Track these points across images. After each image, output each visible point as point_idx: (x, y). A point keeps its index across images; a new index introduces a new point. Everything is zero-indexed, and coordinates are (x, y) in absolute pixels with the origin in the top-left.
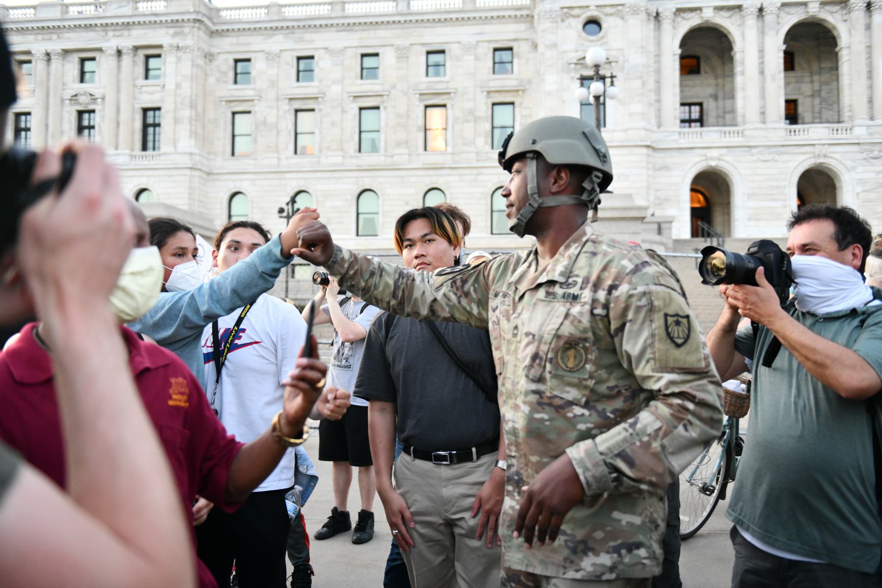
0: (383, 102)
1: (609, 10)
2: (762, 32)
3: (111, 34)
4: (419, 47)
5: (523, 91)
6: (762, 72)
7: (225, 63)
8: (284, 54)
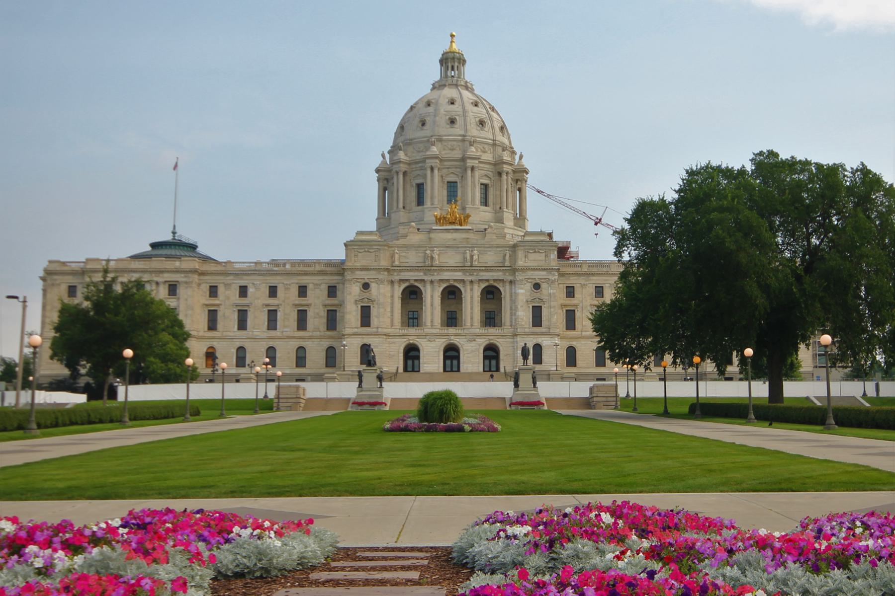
0: (279, 308)
1: (372, 280)
2: (433, 290)
3: (153, 275)
4: (294, 284)
5: (341, 305)
6: (432, 305)
7: (205, 288)
8: (233, 285)
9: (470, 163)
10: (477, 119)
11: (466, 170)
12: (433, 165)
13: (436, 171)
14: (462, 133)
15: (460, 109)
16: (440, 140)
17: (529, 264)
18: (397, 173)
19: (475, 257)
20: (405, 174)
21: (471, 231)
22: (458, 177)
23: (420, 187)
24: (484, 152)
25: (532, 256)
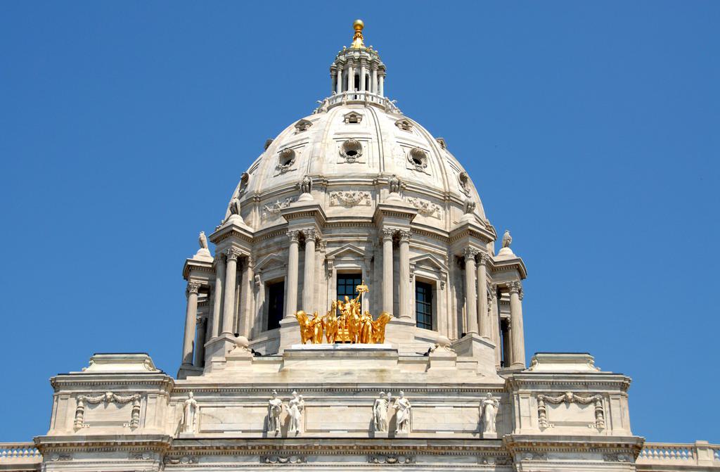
9: (390, 226)
10: (408, 150)
11: (381, 244)
12: (304, 230)
13: (310, 245)
14: (376, 171)
15: (371, 130)
16: (322, 184)
17: (546, 433)
18: (225, 259)
19: (400, 415)
20: (242, 263)
21: (393, 354)
22: (364, 261)
23: (276, 292)
24: (427, 214)
25: (559, 413)
